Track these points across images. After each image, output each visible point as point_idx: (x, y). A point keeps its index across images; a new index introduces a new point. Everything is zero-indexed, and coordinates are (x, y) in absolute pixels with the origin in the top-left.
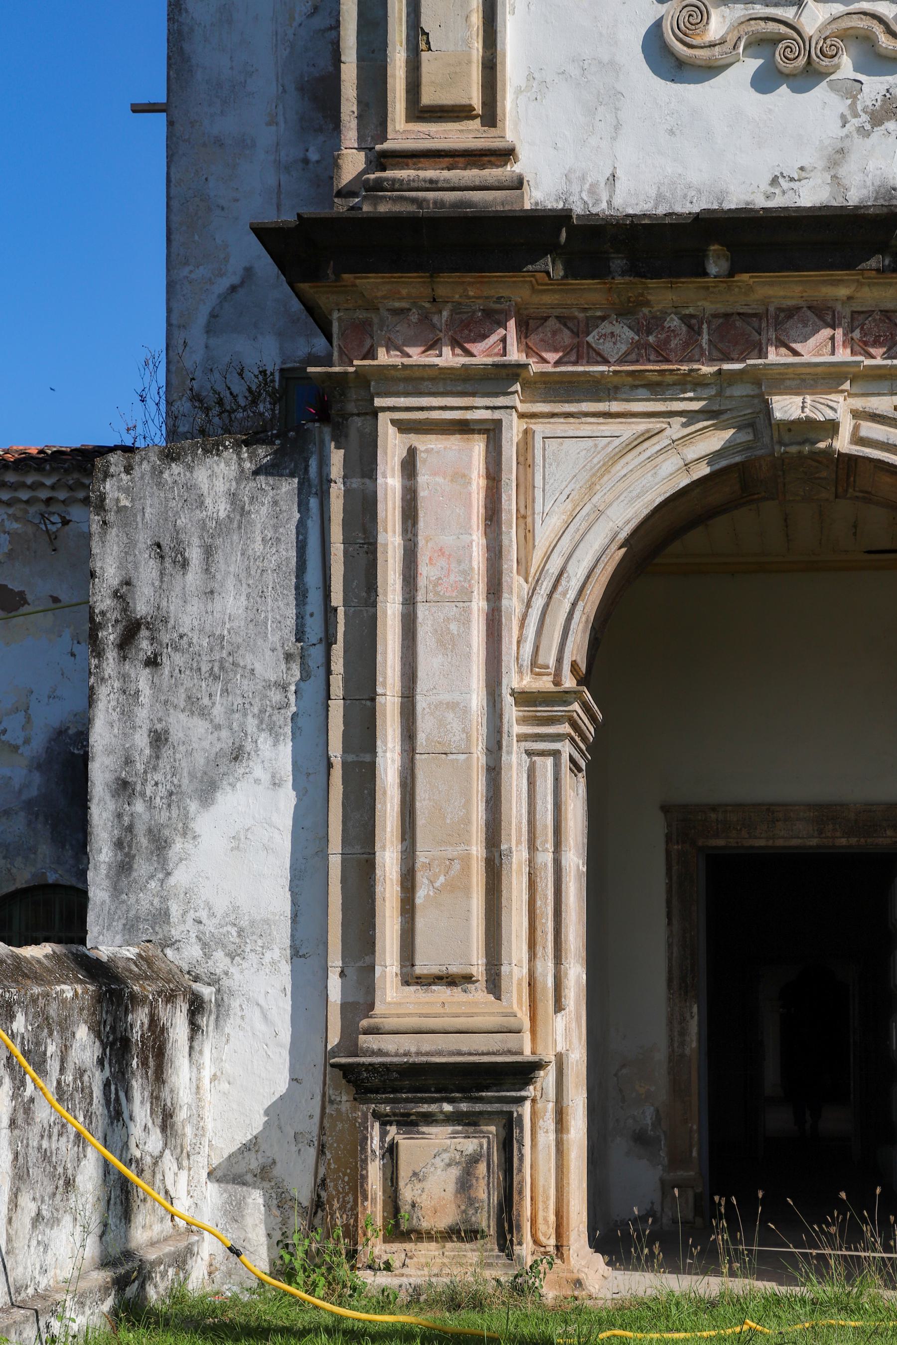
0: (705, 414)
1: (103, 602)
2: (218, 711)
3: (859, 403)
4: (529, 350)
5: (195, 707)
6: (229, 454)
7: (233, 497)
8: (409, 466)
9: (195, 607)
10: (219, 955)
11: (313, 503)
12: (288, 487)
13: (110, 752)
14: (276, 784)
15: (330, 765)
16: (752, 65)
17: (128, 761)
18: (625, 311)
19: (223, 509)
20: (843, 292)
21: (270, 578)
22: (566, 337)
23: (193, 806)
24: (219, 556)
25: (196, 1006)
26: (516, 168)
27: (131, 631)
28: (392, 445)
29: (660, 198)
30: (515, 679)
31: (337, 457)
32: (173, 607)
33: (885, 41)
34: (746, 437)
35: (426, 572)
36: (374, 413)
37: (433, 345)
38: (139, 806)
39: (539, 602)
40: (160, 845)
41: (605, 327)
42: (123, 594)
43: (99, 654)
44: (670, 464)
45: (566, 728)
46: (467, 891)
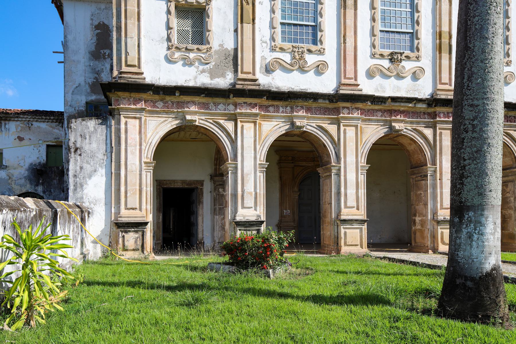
0: (175, 117)
1: (71, 144)
2: (92, 164)
3: (199, 117)
4: (146, 106)
5: (88, 162)
6: (94, 120)
7: (94, 127)
8: (126, 124)
9: (88, 146)
10: (92, 204)
11: (109, 129)
12: (104, 126)
13: (73, 170)
14: (102, 176)
15: (112, 173)
16: (181, 62)
17: (76, 172)
18: (162, 100)
19: (92, 129)
20: (197, 99)
21: (101, 141)
22: (152, 104)
23: (87, 179)
24: (92, 137)
25: (89, 213)
26: (143, 76)
27: (76, 150)
28: (123, 120)
29: (167, 82)
30: (144, 160)
31: (113, 122)
32: (84, 145)
33: (203, 60)
34: (182, 121)
35: (129, 141)
36: (120, 115)
37: (129, 104)
38: (78, 179)
39: (147, 147)
40: (82, 186)
41: (158, 103)
42: (75, 143)
43: (71, 153)
44: (169, 125)
45: (152, 168)
46: (136, 194)
